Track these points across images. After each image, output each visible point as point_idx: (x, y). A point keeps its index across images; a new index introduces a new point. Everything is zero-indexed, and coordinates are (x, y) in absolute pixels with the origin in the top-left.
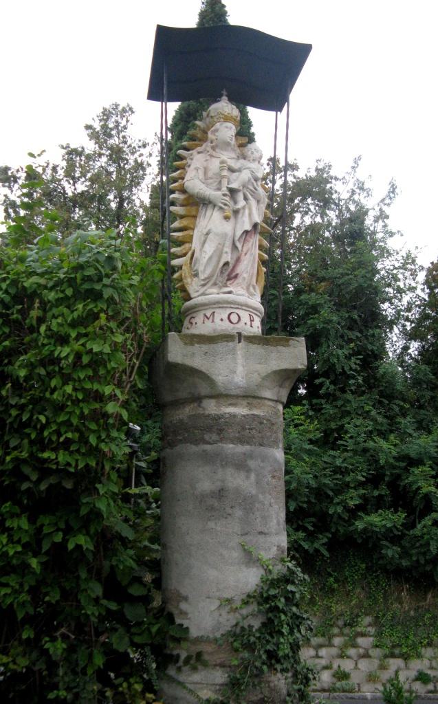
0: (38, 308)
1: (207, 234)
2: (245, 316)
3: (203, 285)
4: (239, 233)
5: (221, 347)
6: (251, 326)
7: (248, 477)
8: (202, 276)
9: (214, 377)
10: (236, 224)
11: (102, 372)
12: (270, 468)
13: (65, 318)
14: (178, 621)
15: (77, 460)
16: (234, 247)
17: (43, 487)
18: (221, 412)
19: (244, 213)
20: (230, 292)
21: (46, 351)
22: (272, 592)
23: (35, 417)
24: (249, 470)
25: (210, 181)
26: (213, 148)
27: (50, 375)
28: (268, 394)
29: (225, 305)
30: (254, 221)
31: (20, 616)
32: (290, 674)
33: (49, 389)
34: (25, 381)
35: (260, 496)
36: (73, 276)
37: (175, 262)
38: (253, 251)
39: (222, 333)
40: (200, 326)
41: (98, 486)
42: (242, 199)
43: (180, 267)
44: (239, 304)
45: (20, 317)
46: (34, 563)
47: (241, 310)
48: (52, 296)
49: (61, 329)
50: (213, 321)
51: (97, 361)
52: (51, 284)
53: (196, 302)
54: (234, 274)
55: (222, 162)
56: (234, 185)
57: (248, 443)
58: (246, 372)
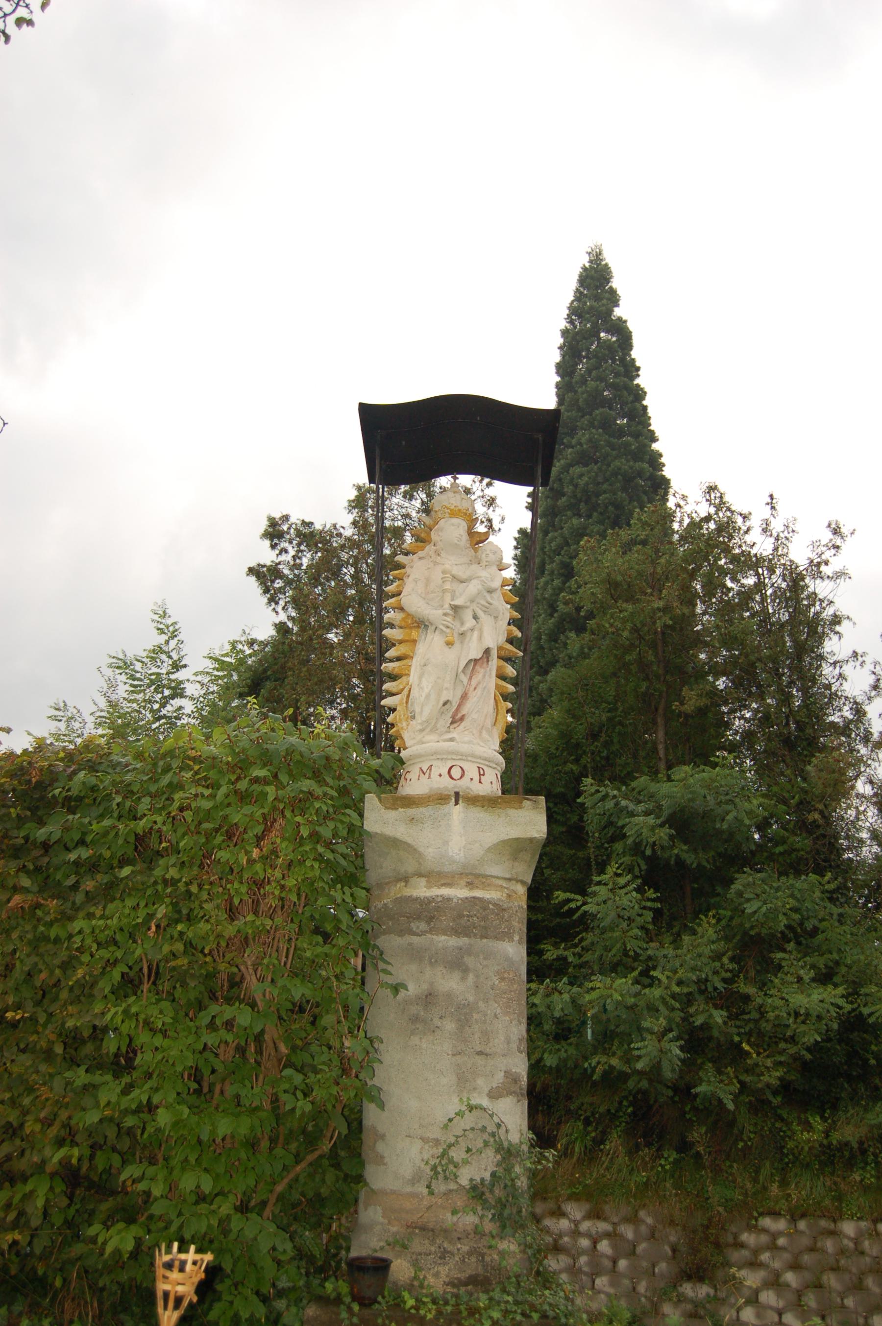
2: (472, 771)
3: (422, 731)
8: (419, 719)
54: (459, 715)
56: (458, 602)
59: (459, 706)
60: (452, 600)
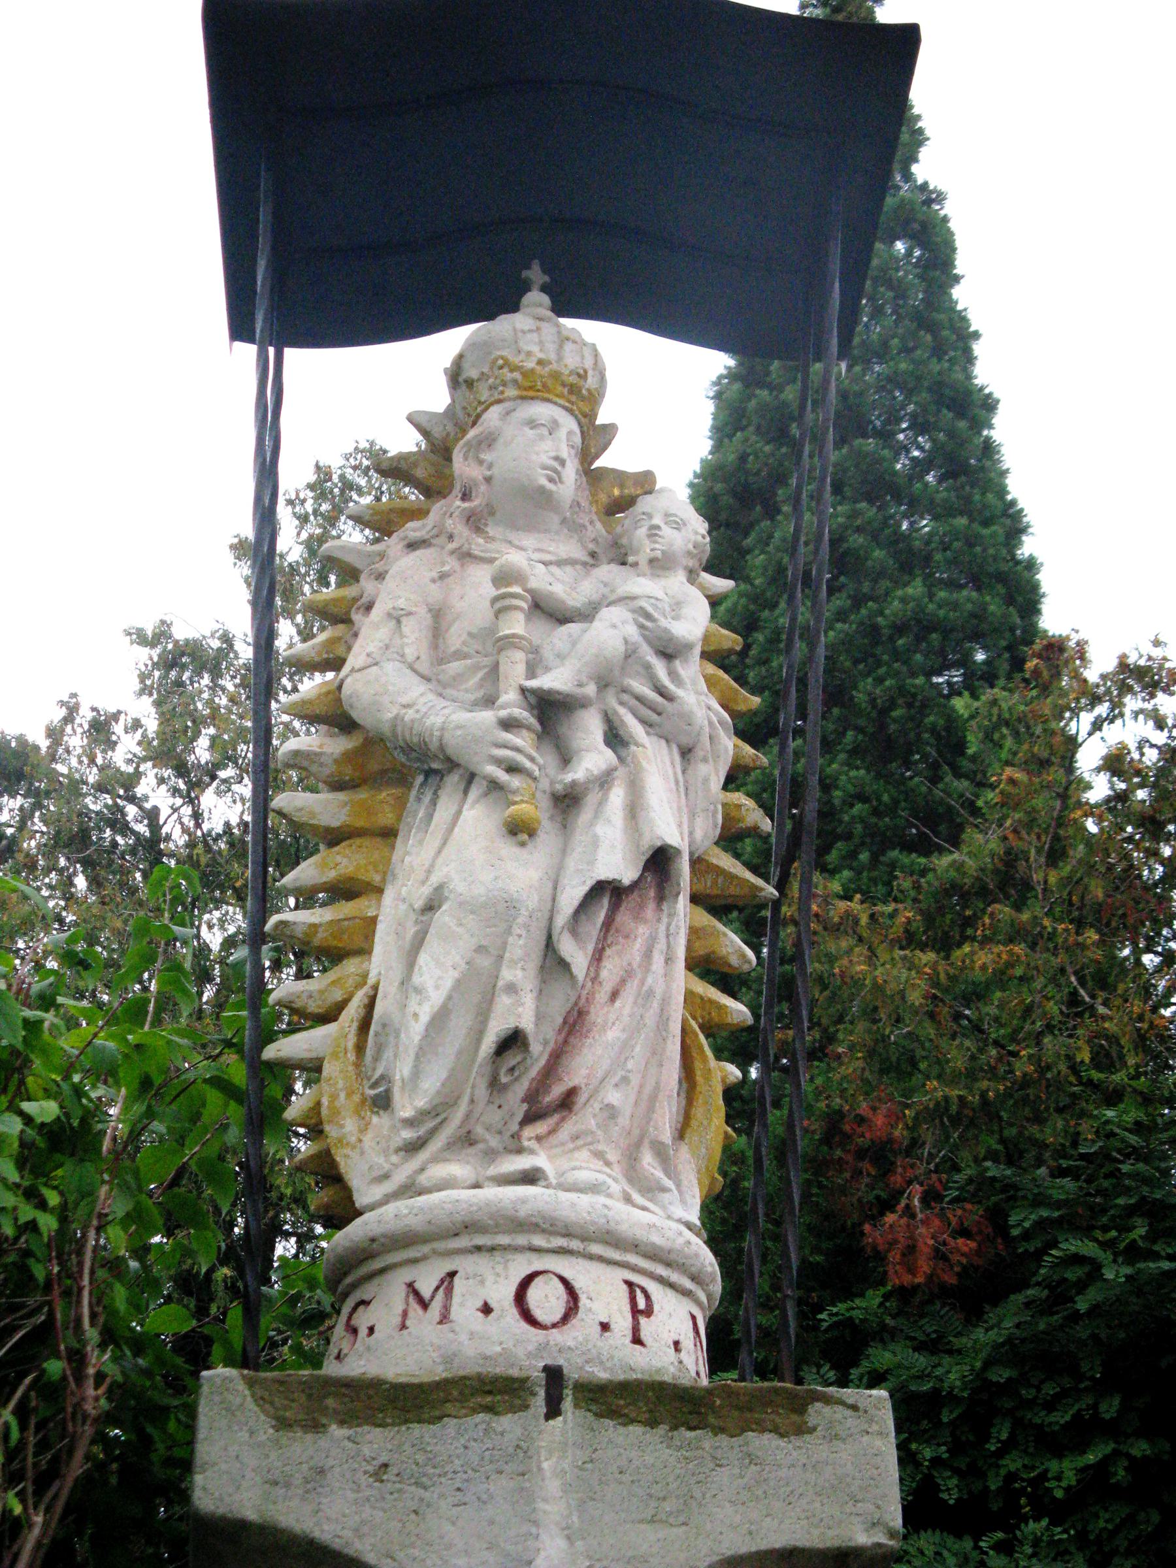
1: (430, 907)
2: (603, 1291)
3: (413, 1148)
4: (573, 894)
5: (456, 1438)
6: (637, 1340)
8: (405, 1107)
10: (564, 851)
16: (553, 962)
19: (601, 803)
20: (530, 1177)
25: (455, 667)
26: (475, 522)
29: (504, 1240)
30: (649, 842)
40: (390, 1342)
43: (313, 1069)
47: (582, 1263)
50: (444, 1318)
54: (557, 1091)
55: (503, 578)
56: (554, 680)
59: (557, 1057)
60: (531, 673)
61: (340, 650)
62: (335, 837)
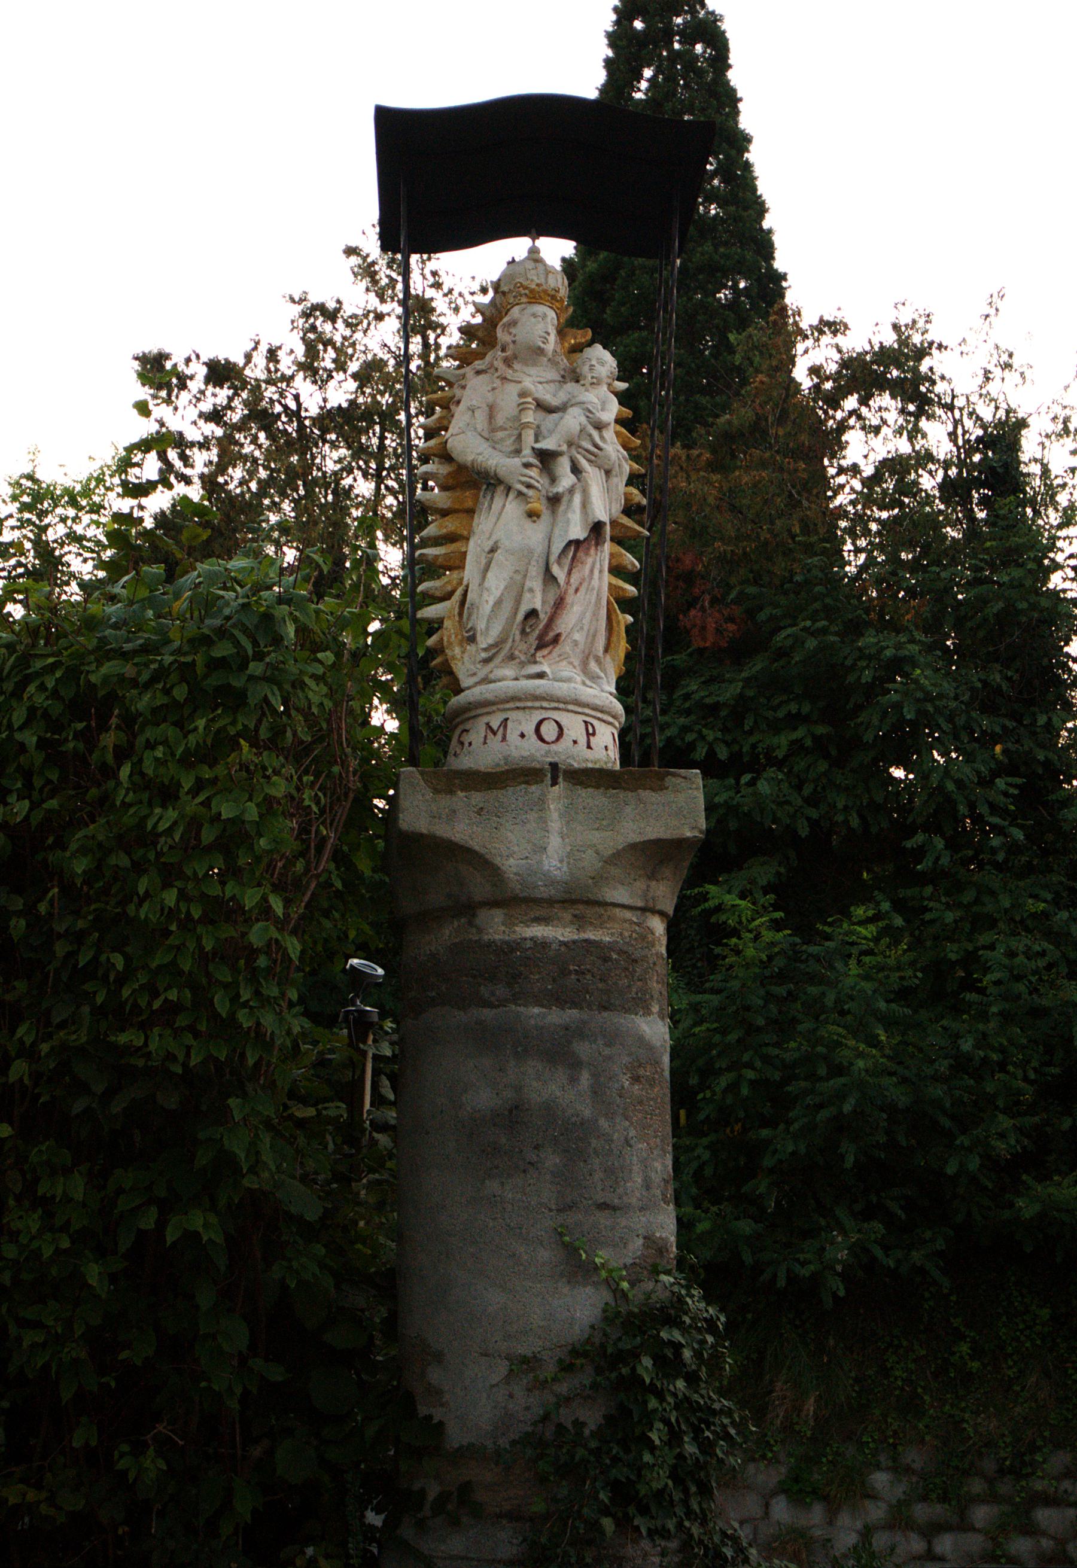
0: (118, 727)
1: (493, 550)
3: (487, 661)
4: (558, 547)
6: (589, 747)
7: (573, 1080)
8: (483, 642)
9: (497, 861)
10: (553, 525)
11: (244, 860)
12: (626, 1059)
13: (170, 747)
14: (423, 1411)
15: (189, 1048)
16: (549, 577)
17: (117, 1107)
18: (514, 936)
19: (570, 501)
20: (541, 675)
21: (129, 819)
22: (626, 1345)
23: (103, 958)
24: (575, 1065)
25: (500, 434)
26: (508, 362)
27: (138, 868)
28: (620, 894)
29: (529, 704)
30: (591, 520)
31: (66, 1395)
32: (673, 1545)
33: (135, 898)
34: (84, 882)
35: (603, 1123)
36: (189, 659)
37: (429, 612)
38: (595, 582)
39: (522, 764)
40: (480, 751)
41: (233, 1102)
42: (568, 469)
43: (440, 622)
44: (573, 698)
45: (81, 746)
46: (93, 1273)
47: (565, 714)
48: (144, 702)
49: (162, 770)
50: (504, 739)
51: (234, 838)
52: (145, 677)
53: (472, 699)
54: (551, 635)
55: (523, 394)
56: (548, 444)
57: (575, 1005)
58: (568, 849)
59: (552, 620)
60: (537, 441)
61: (445, 423)
62: (444, 513)
